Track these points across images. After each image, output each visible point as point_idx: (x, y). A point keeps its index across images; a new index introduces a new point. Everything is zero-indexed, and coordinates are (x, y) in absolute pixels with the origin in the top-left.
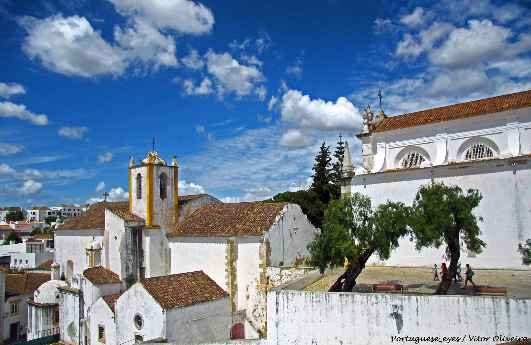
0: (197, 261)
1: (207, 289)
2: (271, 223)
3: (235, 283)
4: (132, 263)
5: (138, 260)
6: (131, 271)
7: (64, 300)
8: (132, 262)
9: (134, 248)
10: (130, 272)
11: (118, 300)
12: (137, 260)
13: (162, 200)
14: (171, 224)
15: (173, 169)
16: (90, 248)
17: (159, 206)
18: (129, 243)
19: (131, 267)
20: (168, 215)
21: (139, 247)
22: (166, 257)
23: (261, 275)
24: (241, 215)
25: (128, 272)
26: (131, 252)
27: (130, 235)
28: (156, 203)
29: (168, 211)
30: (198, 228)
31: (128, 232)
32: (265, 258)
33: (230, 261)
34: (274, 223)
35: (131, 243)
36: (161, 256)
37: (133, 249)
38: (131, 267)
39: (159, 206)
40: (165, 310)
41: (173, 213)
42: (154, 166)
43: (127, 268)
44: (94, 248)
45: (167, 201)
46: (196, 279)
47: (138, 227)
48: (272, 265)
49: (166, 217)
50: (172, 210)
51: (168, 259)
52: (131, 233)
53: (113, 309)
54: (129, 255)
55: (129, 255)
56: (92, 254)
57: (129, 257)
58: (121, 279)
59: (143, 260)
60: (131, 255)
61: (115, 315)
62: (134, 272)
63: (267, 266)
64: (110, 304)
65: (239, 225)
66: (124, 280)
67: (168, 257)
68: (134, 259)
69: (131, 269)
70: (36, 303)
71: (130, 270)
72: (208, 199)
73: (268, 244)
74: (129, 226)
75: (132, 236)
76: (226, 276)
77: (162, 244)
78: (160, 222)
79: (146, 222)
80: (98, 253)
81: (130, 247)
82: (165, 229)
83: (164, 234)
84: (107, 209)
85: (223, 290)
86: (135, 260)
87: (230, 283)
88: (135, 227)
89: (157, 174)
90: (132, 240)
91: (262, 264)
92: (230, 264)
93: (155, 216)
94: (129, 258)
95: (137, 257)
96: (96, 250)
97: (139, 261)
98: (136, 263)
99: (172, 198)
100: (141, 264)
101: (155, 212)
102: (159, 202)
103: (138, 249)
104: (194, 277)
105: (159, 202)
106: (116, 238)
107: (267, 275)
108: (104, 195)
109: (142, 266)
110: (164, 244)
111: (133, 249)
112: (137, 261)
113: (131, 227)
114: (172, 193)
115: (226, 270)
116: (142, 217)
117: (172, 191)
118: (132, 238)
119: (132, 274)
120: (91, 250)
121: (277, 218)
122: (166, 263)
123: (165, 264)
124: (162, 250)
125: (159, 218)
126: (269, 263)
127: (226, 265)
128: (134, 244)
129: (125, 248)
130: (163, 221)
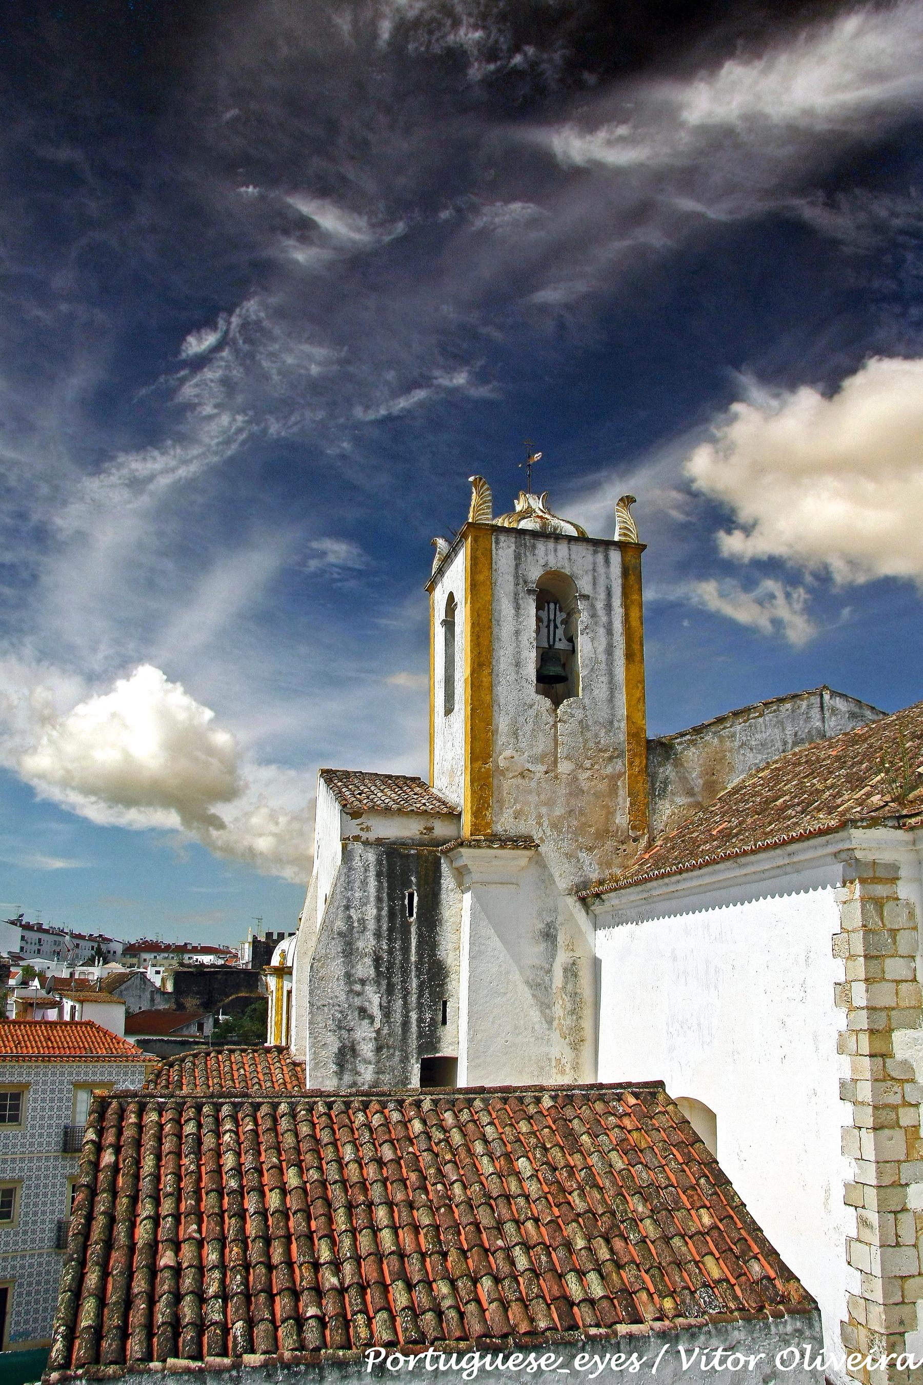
0: (699, 1025)
4: (378, 1032)
5: (414, 1016)
6: (367, 1075)
8: (377, 1025)
9: (390, 952)
10: (360, 1080)
12: (406, 1016)
13: (547, 703)
14: (604, 834)
15: (615, 557)
17: (534, 736)
18: (362, 921)
19: (367, 1049)
20: (585, 785)
21: (419, 947)
22: (573, 1012)
26: (372, 972)
27: (372, 883)
28: (514, 722)
29: (587, 764)
31: (357, 863)
35: (371, 925)
36: (545, 1006)
37: (385, 956)
38: (367, 1049)
39: (534, 736)
41: (620, 775)
42: (502, 538)
45: (579, 714)
47: (421, 844)
49: (576, 791)
50: (611, 758)
51: (587, 1024)
52: (379, 875)
54: (358, 987)
55: (358, 987)
57: (359, 994)
59: (444, 1022)
60: (370, 990)
62: (385, 1078)
67: (587, 1012)
68: (387, 1012)
69: (367, 1062)
71: (361, 1068)
72: (834, 711)
74: (372, 836)
75: (379, 889)
77: (549, 936)
78: (540, 816)
81: (366, 943)
82: (569, 856)
83: (562, 884)
86: (397, 1017)
88: (403, 844)
89: (516, 576)
90: (380, 909)
94: (357, 1001)
95: (405, 998)
97: (420, 1020)
98: (399, 1031)
99: (611, 699)
100: (430, 1040)
101: (502, 763)
102: (532, 712)
103: (413, 958)
105: (532, 712)
109: (436, 1050)
110: (561, 938)
111: (385, 956)
112: (406, 1024)
113: (379, 842)
114: (611, 674)
117: (610, 663)
118: (379, 899)
122: (576, 1046)
123: (567, 1051)
124: (549, 971)
125: (533, 798)
128: (391, 930)
129: (337, 947)
130: (559, 811)
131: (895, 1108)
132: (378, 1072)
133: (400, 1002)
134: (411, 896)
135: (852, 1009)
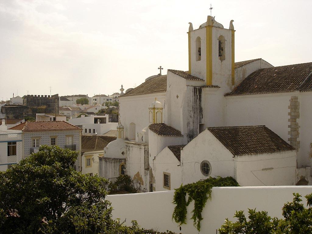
6: (192, 128)
7: (130, 153)
11: (184, 148)
19: (191, 123)
25: (189, 127)
26: (192, 110)
30: (257, 87)
53: (178, 157)
56: (154, 112)
58: (182, 133)
60: (192, 112)
61: (181, 164)
64: (175, 153)
66: (185, 135)
70: (105, 158)
80: (160, 112)
81: (191, 104)
85: (288, 145)
106: (178, 97)
108: (159, 68)
118: (193, 96)
119: (193, 130)
127: (289, 121)
131: (296, 128)
132: (193, 127)
133: (196, 115)
134: (197, 95)
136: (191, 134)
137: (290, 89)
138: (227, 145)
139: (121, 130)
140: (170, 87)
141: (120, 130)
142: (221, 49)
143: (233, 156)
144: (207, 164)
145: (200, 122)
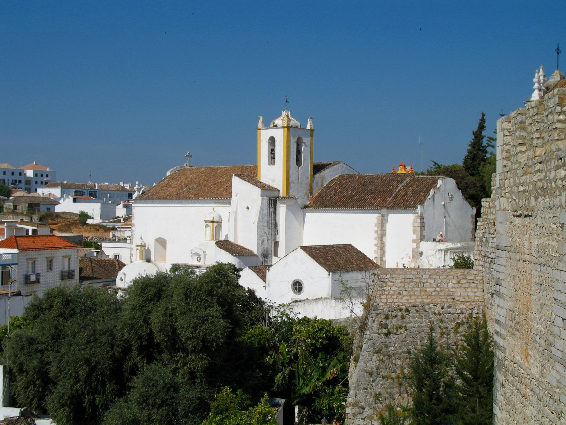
1: (360, 260)
2: (425, 197)
3: (384, 259)
6: (266, 246)
16: (212, 220)
19: (266, 241)
23: (414, 251)
24: (391, 188)
32: (419, 233)
33: (380, 236)
34: (428, 198)
35: (266, 215)
40: (331, 273)
43: (263, 241)
44: (215, 220)
46: (349, 251)
48: (426, 238)
56: (213, 226)
58: (256, 253)
63: (421, 241)
65: (390, 198)
73: (422, 218)
76: (375, 251)
79: (281, 192)
81: (266, 219)
84: (236, 175)
87: (379, 259)
91: (415, 238)
92: (380, 239)
93: (292, 185)
96: (217, 222)
104: (346, 249)
106: (248, 208)
107: (421, 250)
115: (375, 245)
116: (275, 186)
119: (267, 249)
120: (213, 222)
121: (432, 192)
126: (422, 238)
135: (378, 234)
136: (265, 253)
137: (377, 206)
138: (320, 263)
139: (143, 248)
140: (236, 196)
141: (141, 249)
142: (299, 152)
143: (328, 273)
144: (299, 282)
145: (275, 239)
